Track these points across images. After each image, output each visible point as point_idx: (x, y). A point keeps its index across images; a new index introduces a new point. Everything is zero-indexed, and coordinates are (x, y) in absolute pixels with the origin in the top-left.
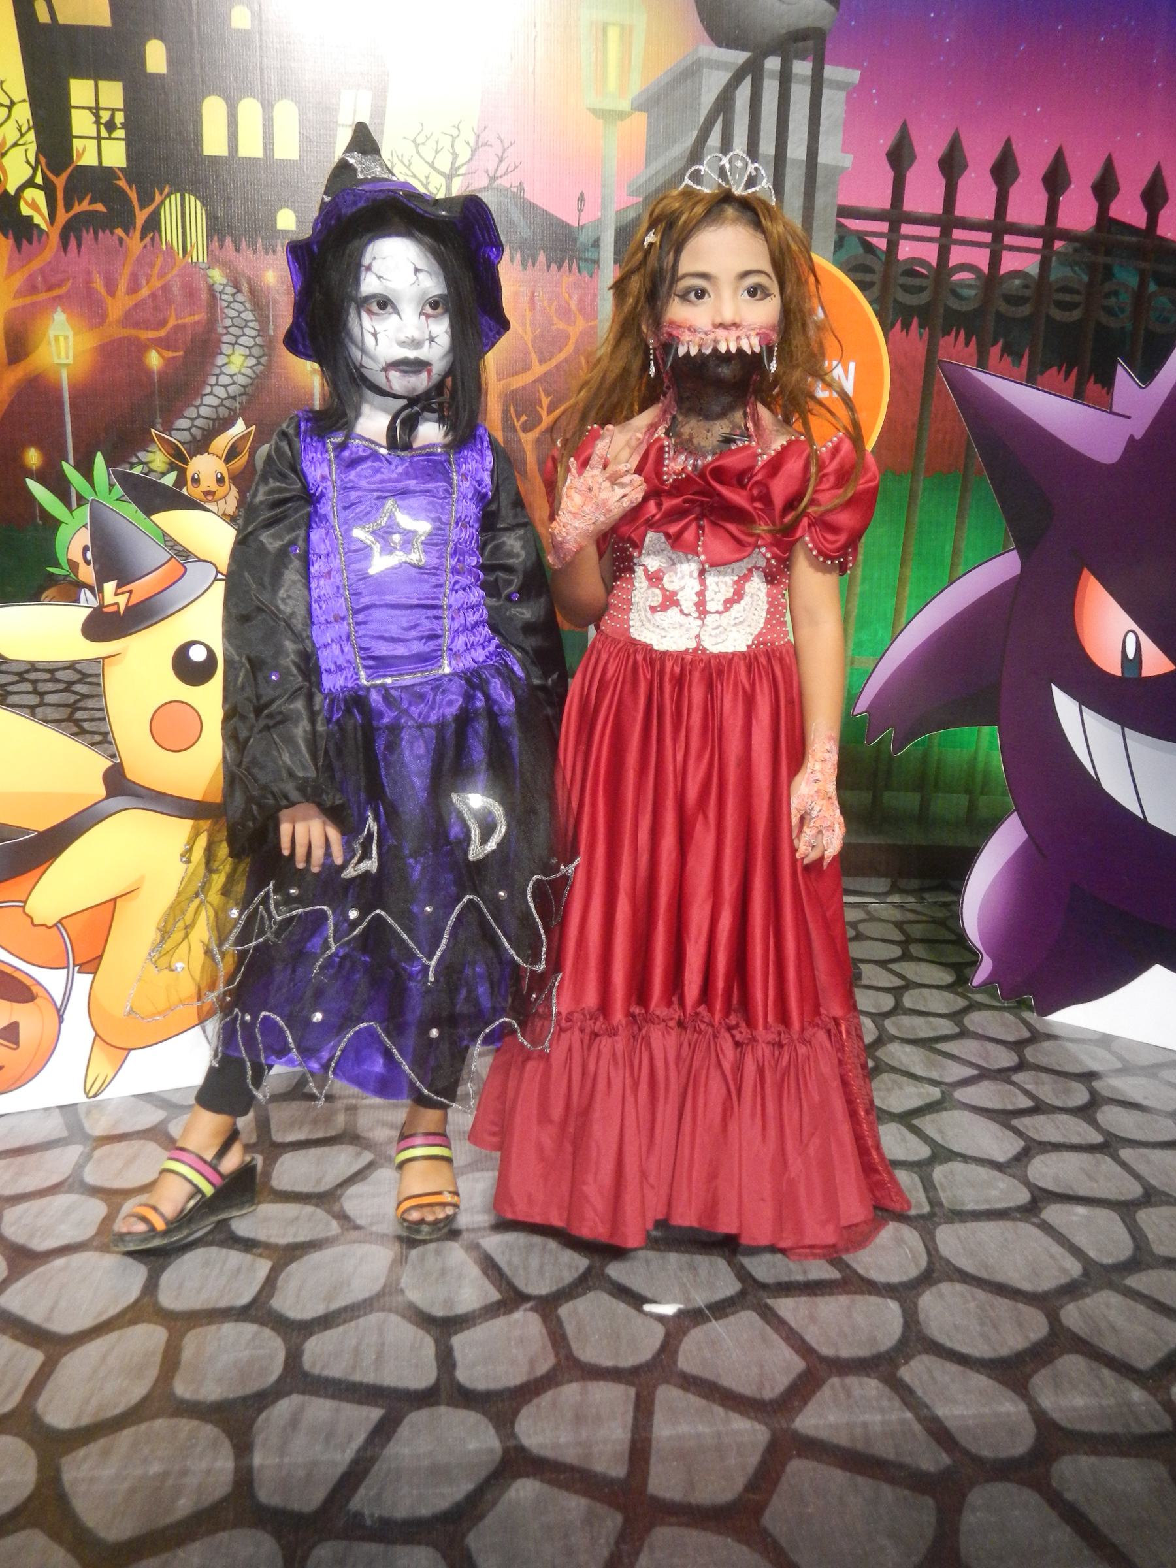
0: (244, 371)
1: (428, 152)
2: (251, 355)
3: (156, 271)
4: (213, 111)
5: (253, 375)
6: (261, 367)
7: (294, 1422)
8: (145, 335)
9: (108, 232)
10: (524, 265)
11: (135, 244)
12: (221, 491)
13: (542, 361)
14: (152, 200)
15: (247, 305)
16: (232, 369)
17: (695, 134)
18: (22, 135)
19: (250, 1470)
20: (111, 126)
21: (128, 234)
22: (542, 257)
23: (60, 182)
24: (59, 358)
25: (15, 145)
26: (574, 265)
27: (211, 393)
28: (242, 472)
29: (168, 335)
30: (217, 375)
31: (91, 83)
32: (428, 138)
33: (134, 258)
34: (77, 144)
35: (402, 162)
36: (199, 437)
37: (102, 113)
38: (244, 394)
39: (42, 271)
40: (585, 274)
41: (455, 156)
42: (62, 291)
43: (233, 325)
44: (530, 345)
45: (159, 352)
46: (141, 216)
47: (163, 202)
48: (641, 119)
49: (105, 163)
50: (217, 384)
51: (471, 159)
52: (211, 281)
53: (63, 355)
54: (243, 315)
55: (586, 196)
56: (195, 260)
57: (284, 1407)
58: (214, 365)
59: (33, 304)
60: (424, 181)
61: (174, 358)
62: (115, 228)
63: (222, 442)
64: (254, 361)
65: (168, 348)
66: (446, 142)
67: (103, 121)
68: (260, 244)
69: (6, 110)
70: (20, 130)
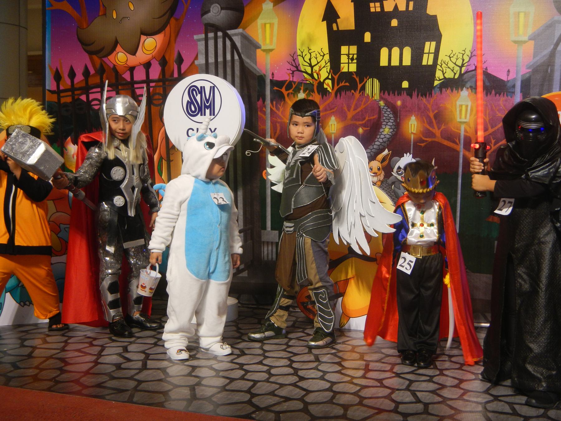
0: (389, 133)
1: (454, 60)
2: (391, 128)
3: (363, 103)
4: (384, 52)
5: (392, 135)
6: (394, 132)
7: (358, 409)
8: (358, 123)
9: (349, 91)
10: (487, 95)
11: (357, 95)
12: (379, 173)
13: (492, 128)
14: (363, 81)
15: (391, 112)
16: (385, 133)
17: (552, 47)
18: (326, 64)
19: (346, 413)
20: (352, 59)
21: (355, 92)
22: (493, 92)
23: (336, 77)
24: (332, 131)
25: (324, 67)
26: (505, 93)
27: (378, 141)
28: (386, 166)
29: (366, 122)
30: (380, 135)
31: (348, 46)
32: (454, 55)
33: (357, 98)
34: (342, 65)
35: (445, 63)
36: (373, 155)
37: (350, 55)
38: (388, 141)
39: (329, 104)
40: (509, 97)
41: (463, 60)
42: (335, 109)
43: (386, 119)
44: (488, 122)
45: (362, 128)
46: (360, 86)
47: (367, 81)
48: (532, 42)
49: (350, 71)
50: (380, 138)
51: (469, 61)
52: (380, 105)
53: (333, 130)
54: (389, 116)
55: (510, 70)
56: (375, 99)
57: (356, 407)
58: (379, 132)
59: (325, 115)
60: (452, 69)
61: (367, 130)
62: (351, 90)
63: (380, 157)
64: (392, 130)
65: (365, 127)
66: (460, 56)
67: (350, 58)
68: (396, 93)
69: (322, 57)
70: (325, 62)
